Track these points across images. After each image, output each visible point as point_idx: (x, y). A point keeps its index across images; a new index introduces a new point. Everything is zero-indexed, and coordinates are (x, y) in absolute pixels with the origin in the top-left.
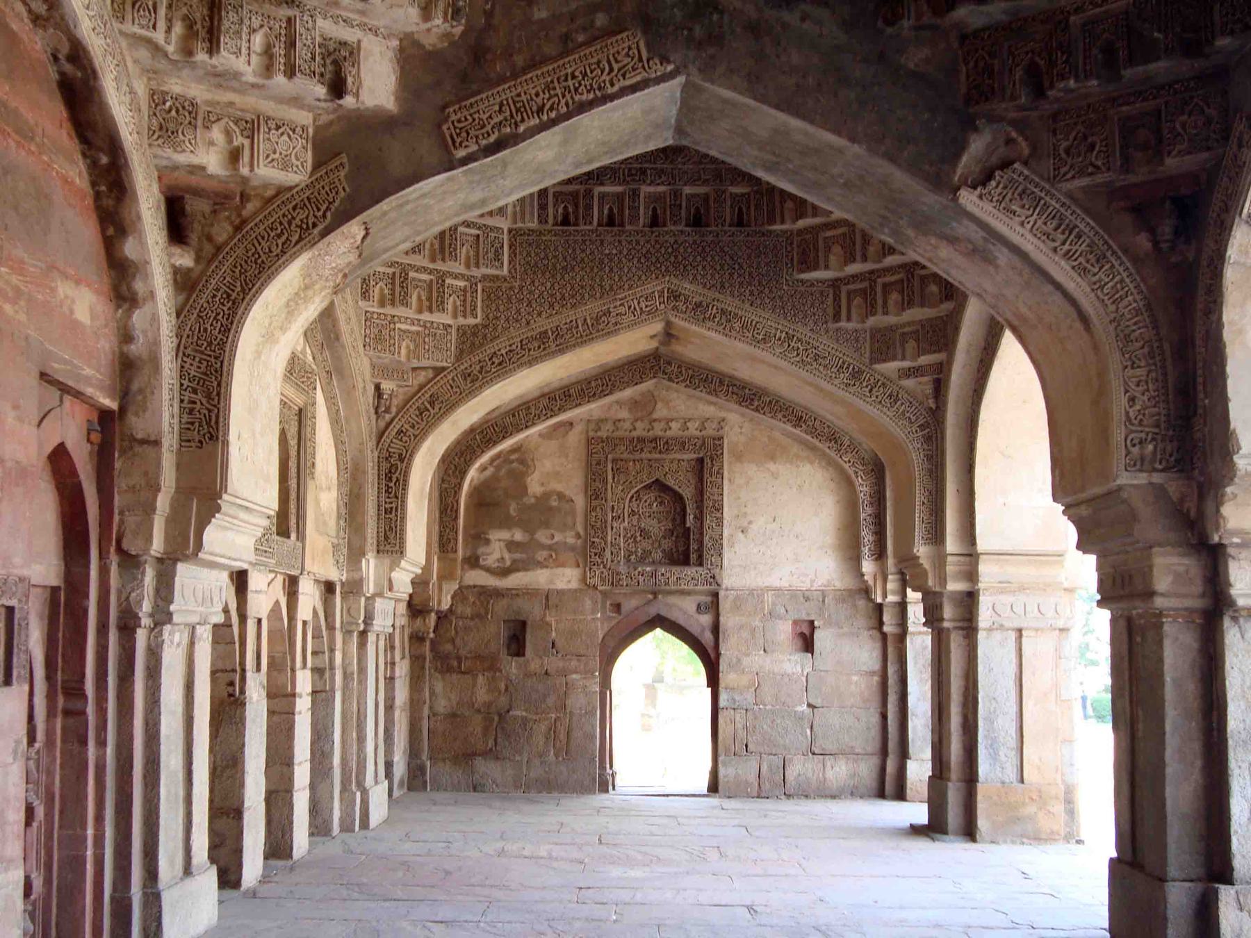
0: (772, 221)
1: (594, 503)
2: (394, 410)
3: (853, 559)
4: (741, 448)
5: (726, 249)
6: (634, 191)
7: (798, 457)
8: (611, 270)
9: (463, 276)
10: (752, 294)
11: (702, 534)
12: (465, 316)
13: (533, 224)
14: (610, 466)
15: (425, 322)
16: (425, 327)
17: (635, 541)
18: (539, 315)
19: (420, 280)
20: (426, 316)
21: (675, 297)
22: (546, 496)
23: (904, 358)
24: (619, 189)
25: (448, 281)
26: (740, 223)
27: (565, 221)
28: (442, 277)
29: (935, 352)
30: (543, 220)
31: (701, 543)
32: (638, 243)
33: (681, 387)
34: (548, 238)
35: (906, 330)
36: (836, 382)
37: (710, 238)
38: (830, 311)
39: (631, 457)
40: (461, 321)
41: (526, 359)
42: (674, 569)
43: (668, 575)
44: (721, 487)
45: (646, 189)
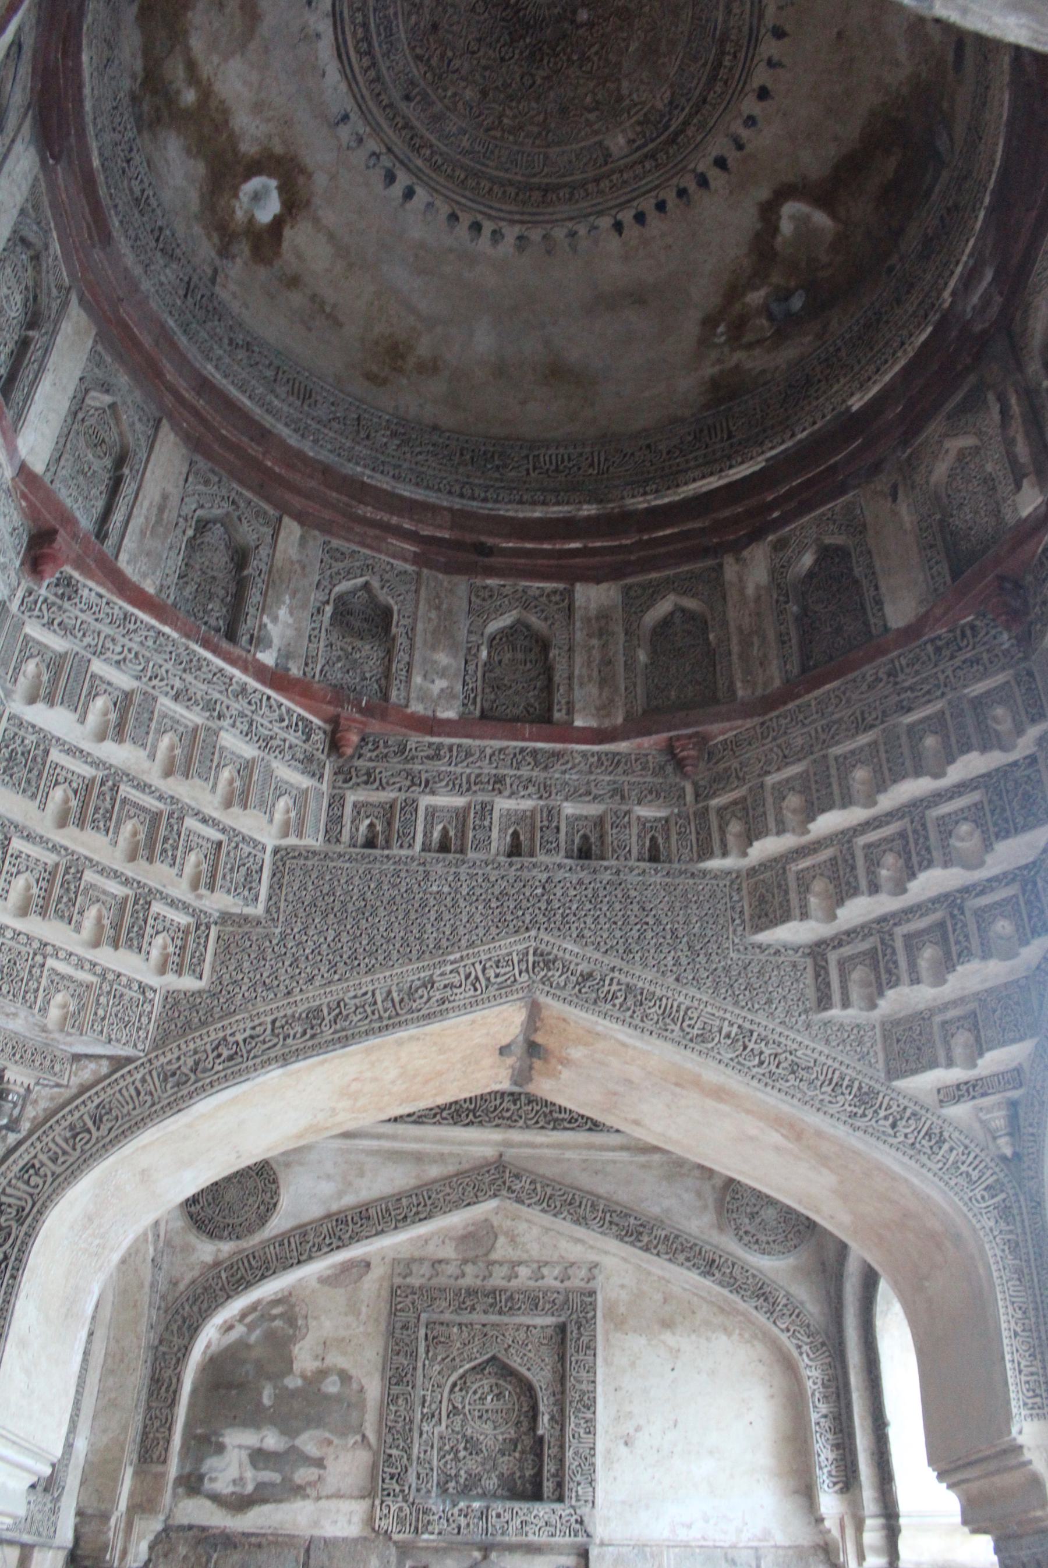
0: (705, 852)
1: (396, 1390)
2: (26, 1126)
3: (806, 1492)
4: (622, 1309)
5: (633, 893)
6: (484, 806)
7: (707, 1323)
8: (439, 918)
9: (185, 907)
10: (677, 962)
11: (562, 1447)
12: (179, 972)
13: (313, 841)
14: (422, 1332)
15: (105, 971)
16: (104, 977)
17: (456, 1459)
18: (311, 980)
19: (104, 892)
20: (107, 957)
21: (546, 964)
22: (323, 1374)
23: (950, 1063)
24: (460, 801)
25: (157, 907)
26: (654, 857)
27: (370, 843)
28: (145, 897)
29: (1013, 1041)
30: (332, 834)
31: (561, 1461)
32: (486, 879)
33: (534, 1213)
34: (339, 864)
35: (951, 1014)
36: (833, 1109)
37: (607, 876)
38: (811, 993)
39: (458, 1319)
40: (173, 982)
41: (278, 1051)
42: (517, 1506)
43: (507, 1516)
44: (592, 1370)
45: (503, 804)
